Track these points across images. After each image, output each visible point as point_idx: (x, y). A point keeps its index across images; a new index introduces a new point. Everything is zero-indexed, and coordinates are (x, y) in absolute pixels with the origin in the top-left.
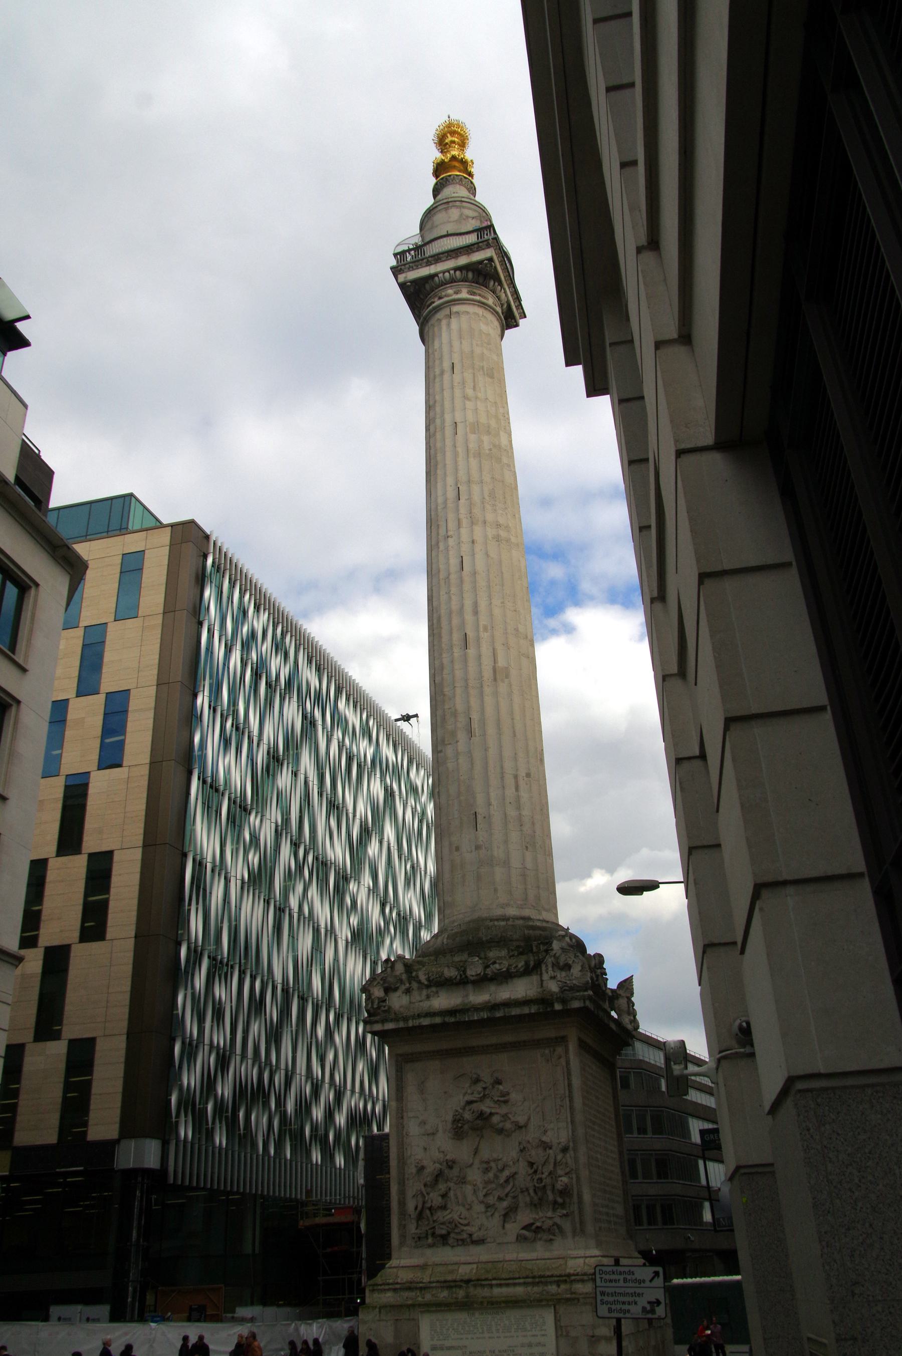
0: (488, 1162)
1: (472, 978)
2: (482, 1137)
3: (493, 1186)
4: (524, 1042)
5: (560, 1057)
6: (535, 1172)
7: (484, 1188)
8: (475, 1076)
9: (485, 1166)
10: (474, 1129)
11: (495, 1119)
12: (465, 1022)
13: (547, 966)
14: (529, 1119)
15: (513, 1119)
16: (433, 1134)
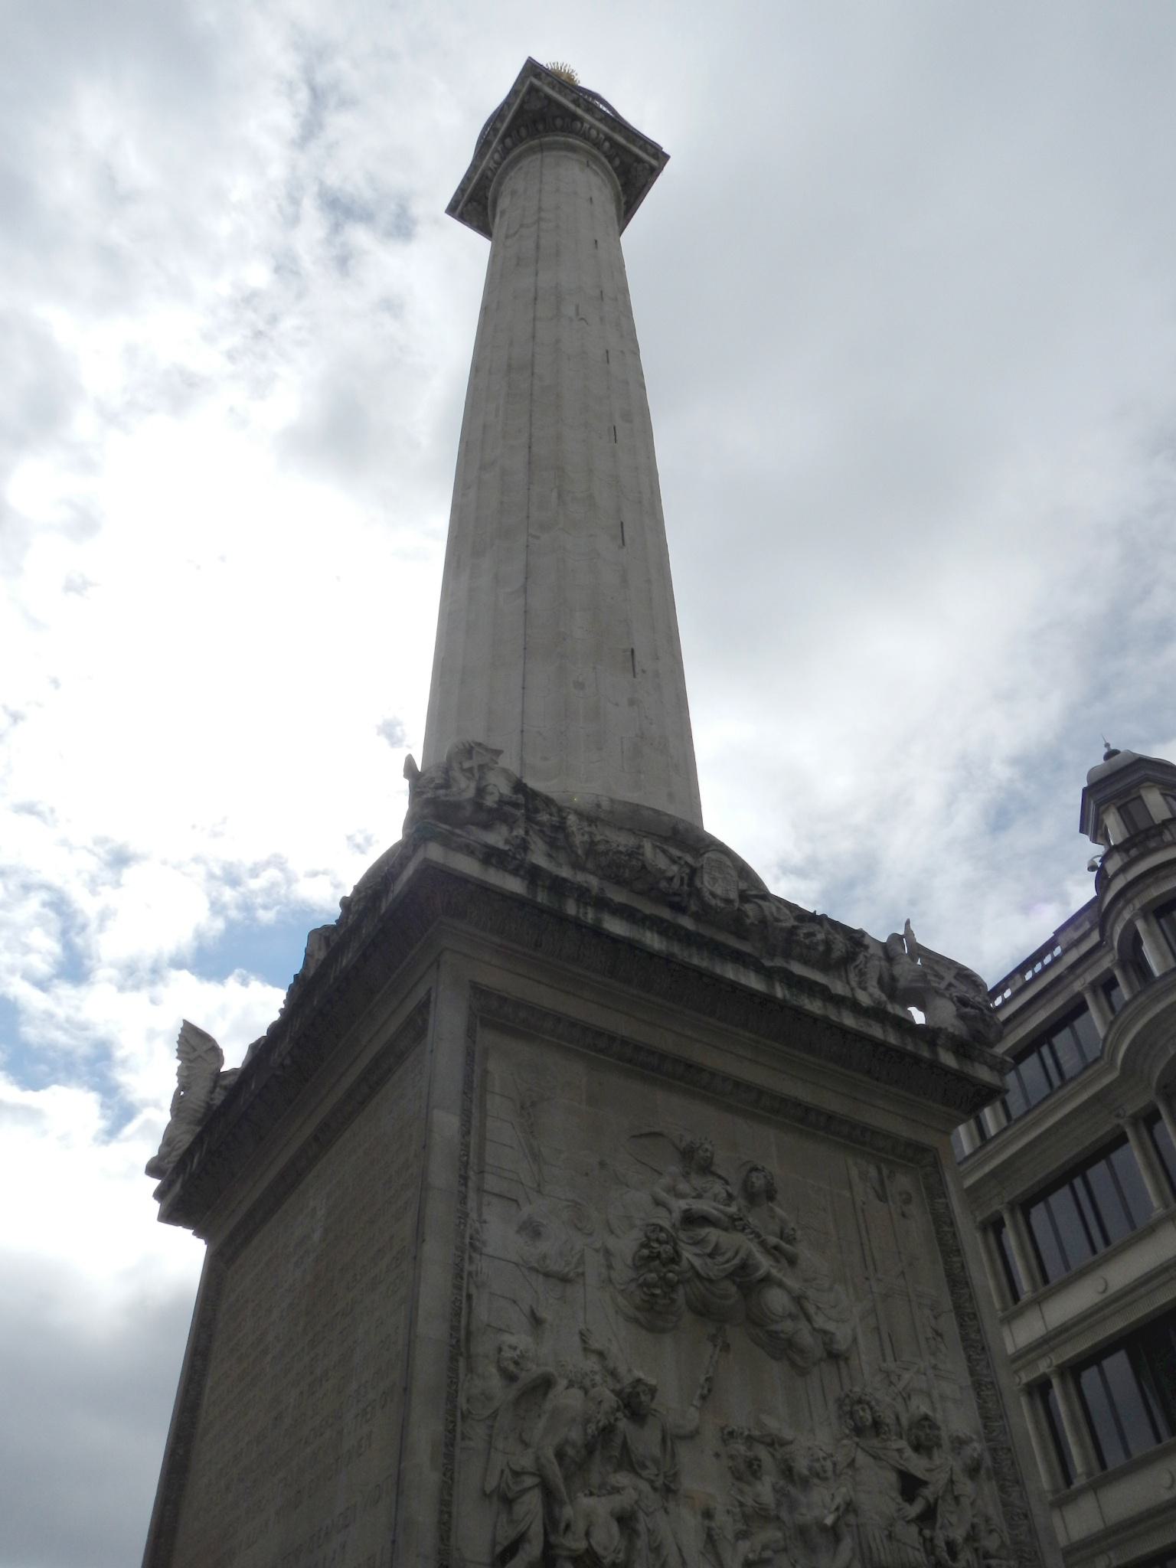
0: (750, 1440)
1: (713, 902)
2: (726, 1348)
3: (770, 1534)
4: (830, 1117)
5: (908, 1201)
6: (928, 1516)
7: (742, 1535)
8: (709, 1147)
9: (740, 1448)
10: (703, 1311)
11: (776, 1300)
12: (719, 980)
13: (862, 974)
14: (855, 1340)
15: (820, 1322)
16: (564, 1280)
